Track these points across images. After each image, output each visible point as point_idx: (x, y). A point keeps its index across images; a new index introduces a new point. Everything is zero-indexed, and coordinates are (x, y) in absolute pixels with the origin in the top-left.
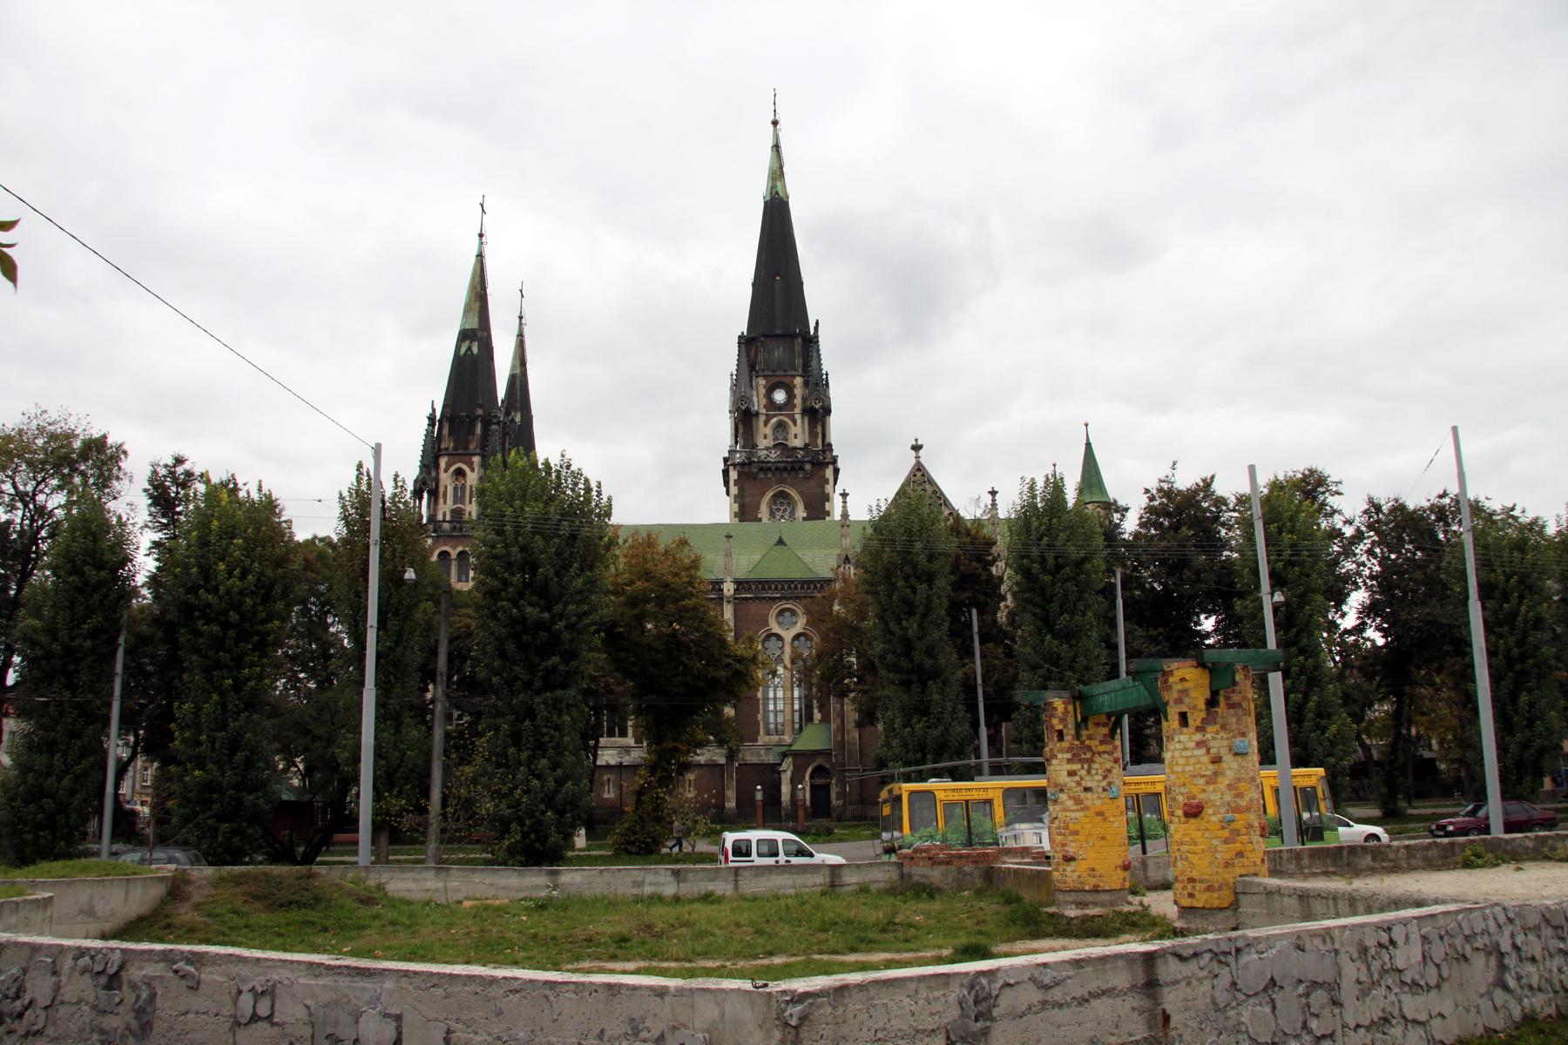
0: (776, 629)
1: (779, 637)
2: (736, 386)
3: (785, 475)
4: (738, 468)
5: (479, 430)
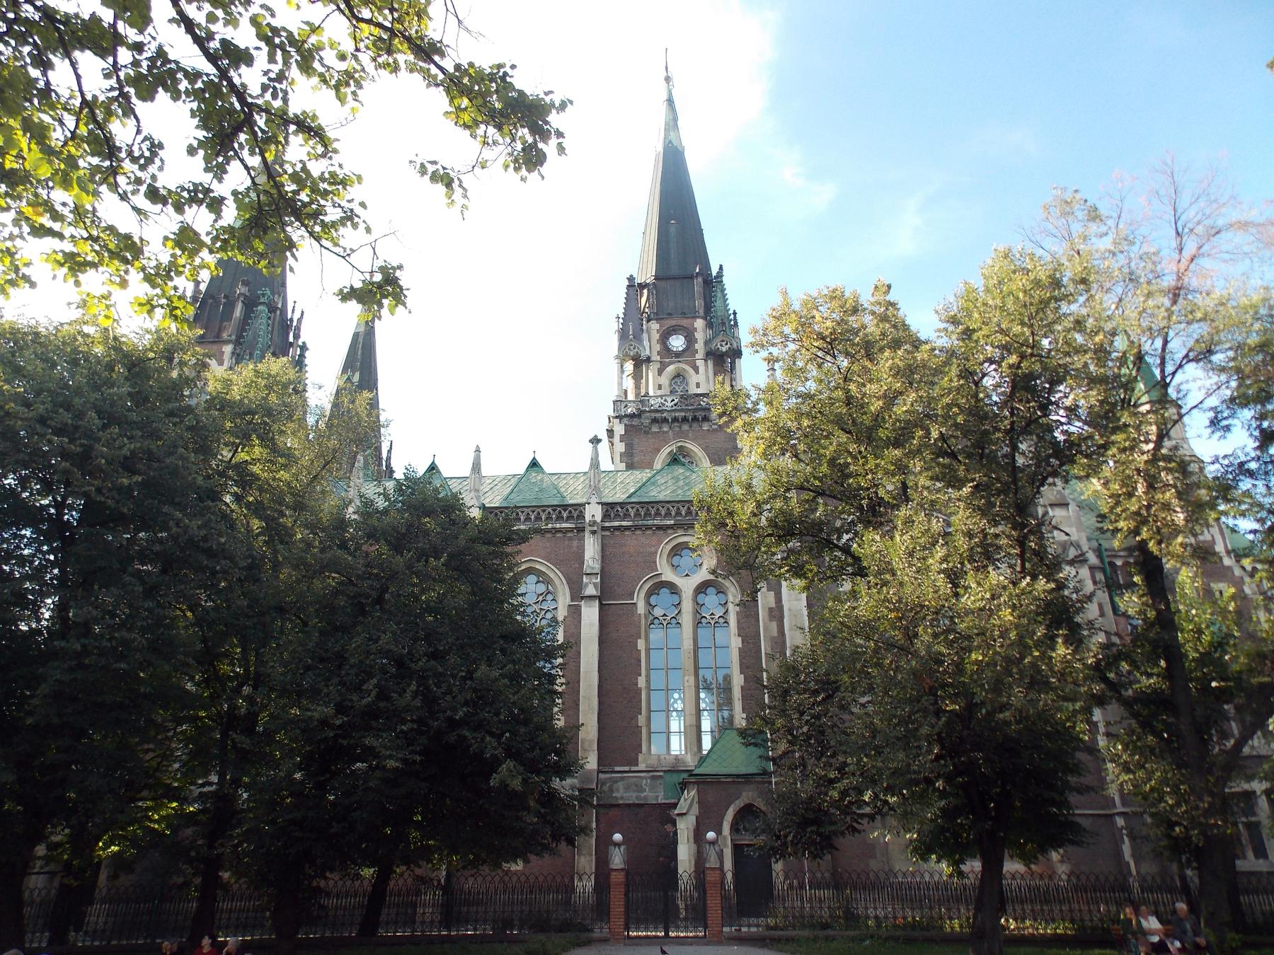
0: (668, 575)
1: (673, 589)
2: (623, 335)
3: (685, 427)
4: (626, 421)
5: (238, 311)
